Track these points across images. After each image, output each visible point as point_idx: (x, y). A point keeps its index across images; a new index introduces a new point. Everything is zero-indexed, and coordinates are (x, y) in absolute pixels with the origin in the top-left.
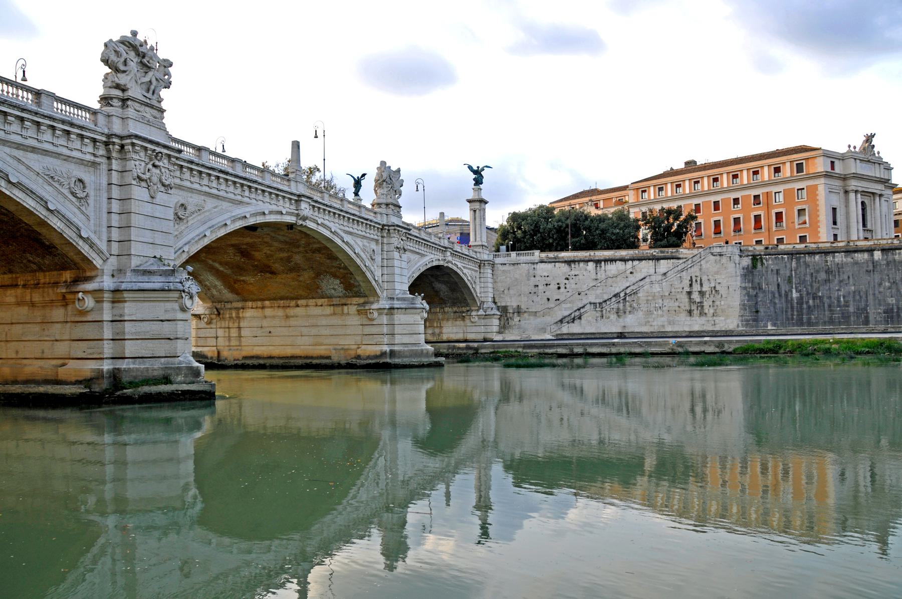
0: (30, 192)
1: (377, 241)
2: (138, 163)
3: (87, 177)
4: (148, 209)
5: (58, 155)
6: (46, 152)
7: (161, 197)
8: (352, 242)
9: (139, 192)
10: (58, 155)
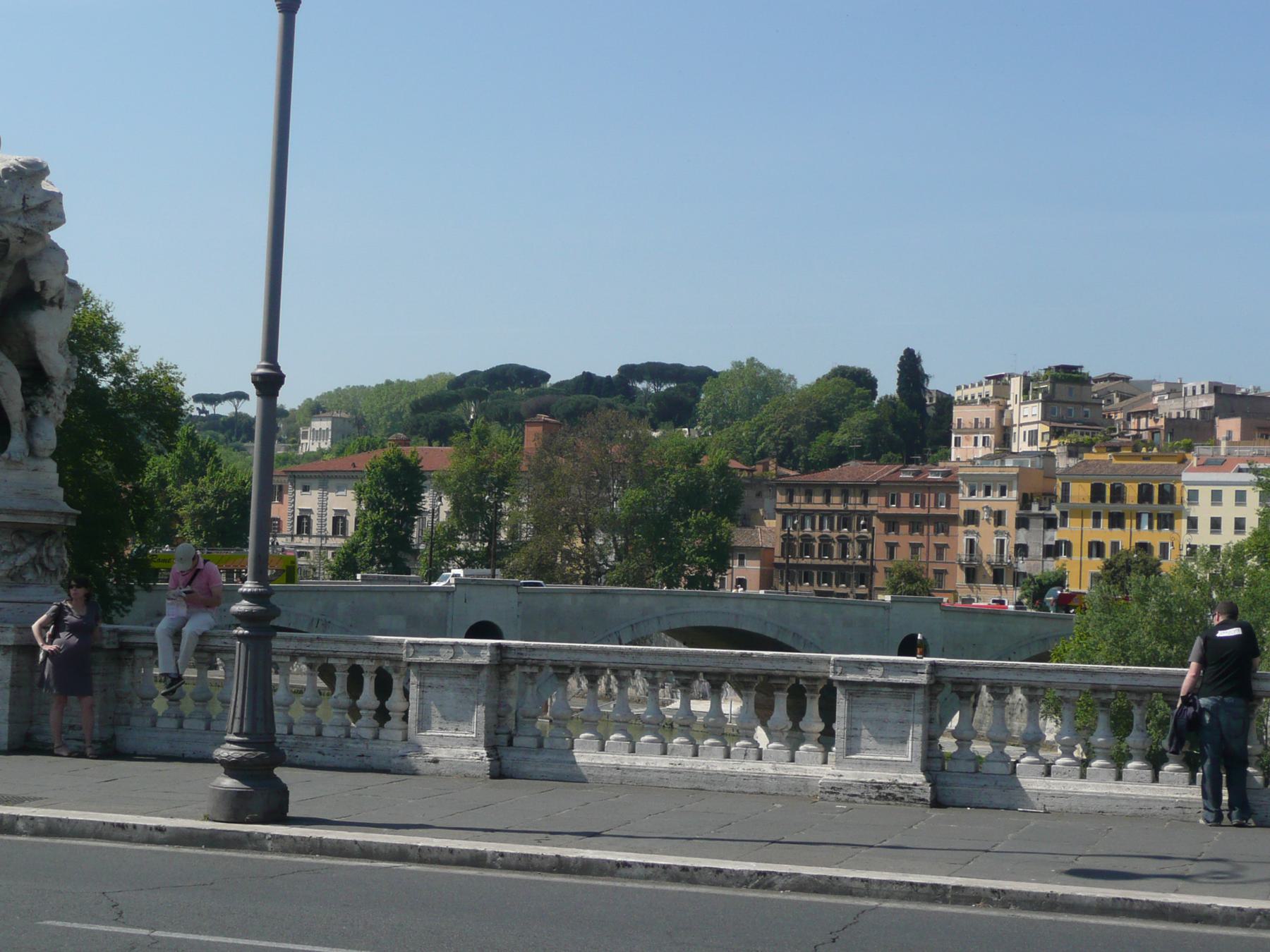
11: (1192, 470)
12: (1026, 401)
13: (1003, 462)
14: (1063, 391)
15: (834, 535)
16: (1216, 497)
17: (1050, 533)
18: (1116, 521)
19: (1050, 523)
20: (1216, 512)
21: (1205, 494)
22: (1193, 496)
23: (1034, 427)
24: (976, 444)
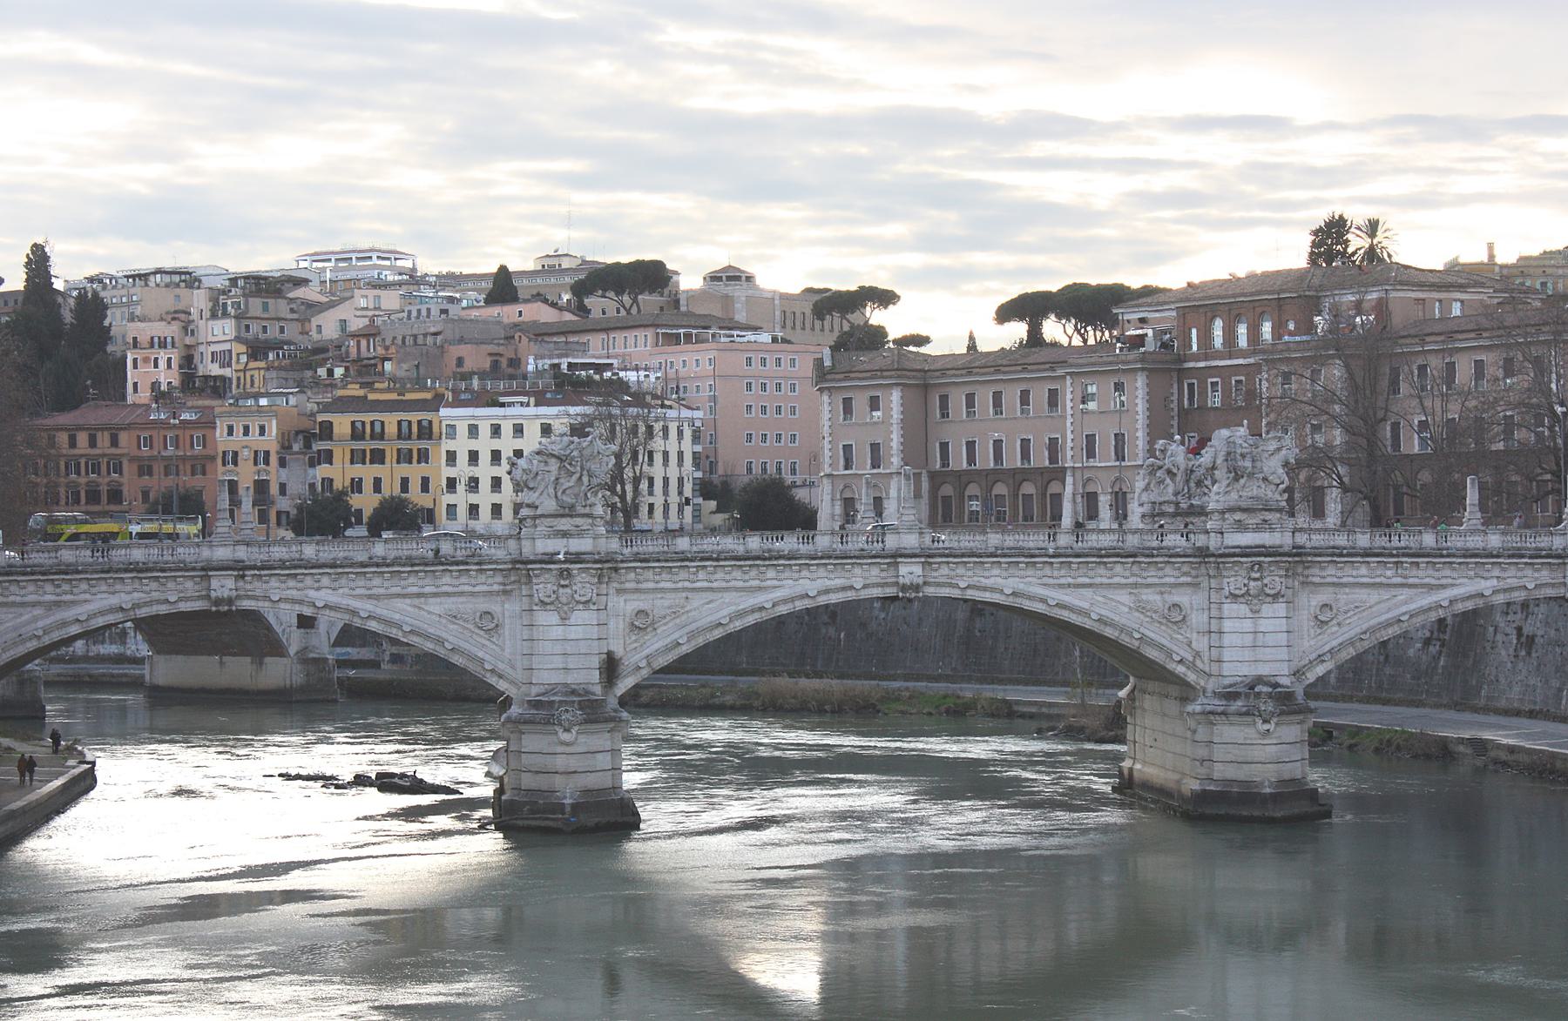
0: (427, 637)
1: (1196, 585)
2: (544, 586)
3: (495, 608)
4: (558, 632)
5: (462, 594)
6: (447, 594)
7: (580, 616)
8: (1085, 605)
9: (547, 618)
10: (462, 594)
11: (449, 405)
12: (214, 316)
13: (257, 401)
14: (255, 306)
15: (83, 480)
16: (473, 431)
17: (311, 471)
18: (378, 457)
19: (313, 464)
20: (473, 445)
21: (462, 429)
22: (452, 432)
23: (227, 346)
24: (156, 366)
